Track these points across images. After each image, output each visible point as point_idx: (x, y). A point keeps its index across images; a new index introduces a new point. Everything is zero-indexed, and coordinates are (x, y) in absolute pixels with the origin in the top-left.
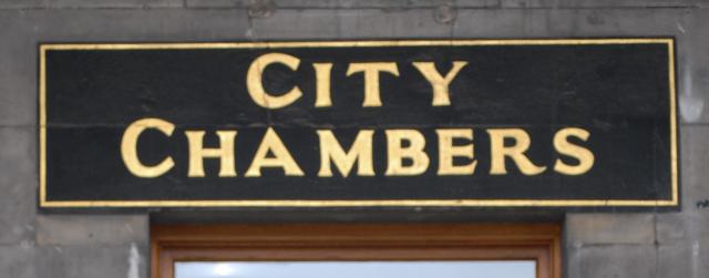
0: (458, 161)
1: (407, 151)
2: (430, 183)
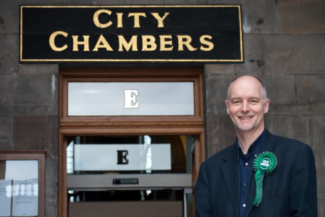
0: (167, 46)
1: (149, 43)
2: (157, 53)
